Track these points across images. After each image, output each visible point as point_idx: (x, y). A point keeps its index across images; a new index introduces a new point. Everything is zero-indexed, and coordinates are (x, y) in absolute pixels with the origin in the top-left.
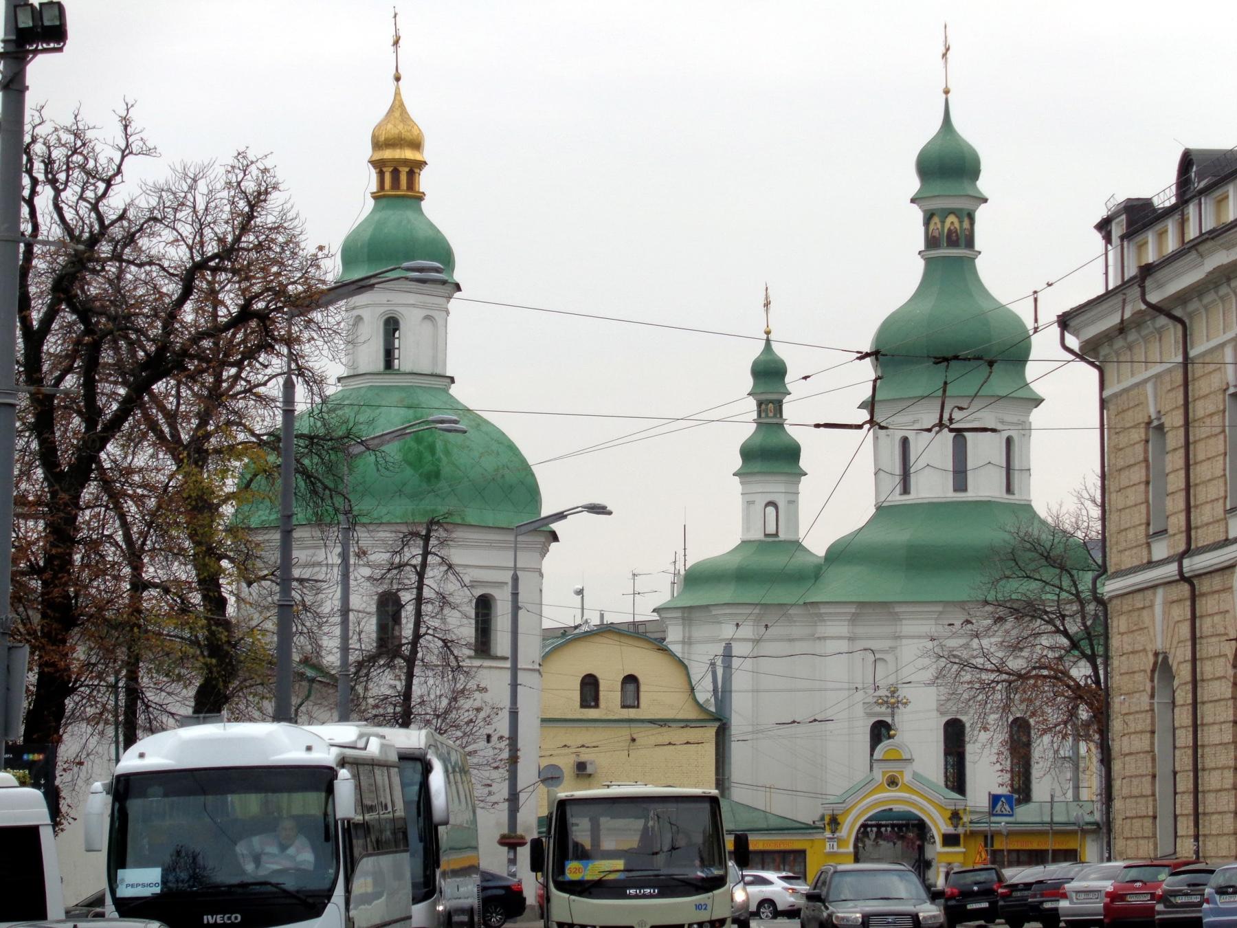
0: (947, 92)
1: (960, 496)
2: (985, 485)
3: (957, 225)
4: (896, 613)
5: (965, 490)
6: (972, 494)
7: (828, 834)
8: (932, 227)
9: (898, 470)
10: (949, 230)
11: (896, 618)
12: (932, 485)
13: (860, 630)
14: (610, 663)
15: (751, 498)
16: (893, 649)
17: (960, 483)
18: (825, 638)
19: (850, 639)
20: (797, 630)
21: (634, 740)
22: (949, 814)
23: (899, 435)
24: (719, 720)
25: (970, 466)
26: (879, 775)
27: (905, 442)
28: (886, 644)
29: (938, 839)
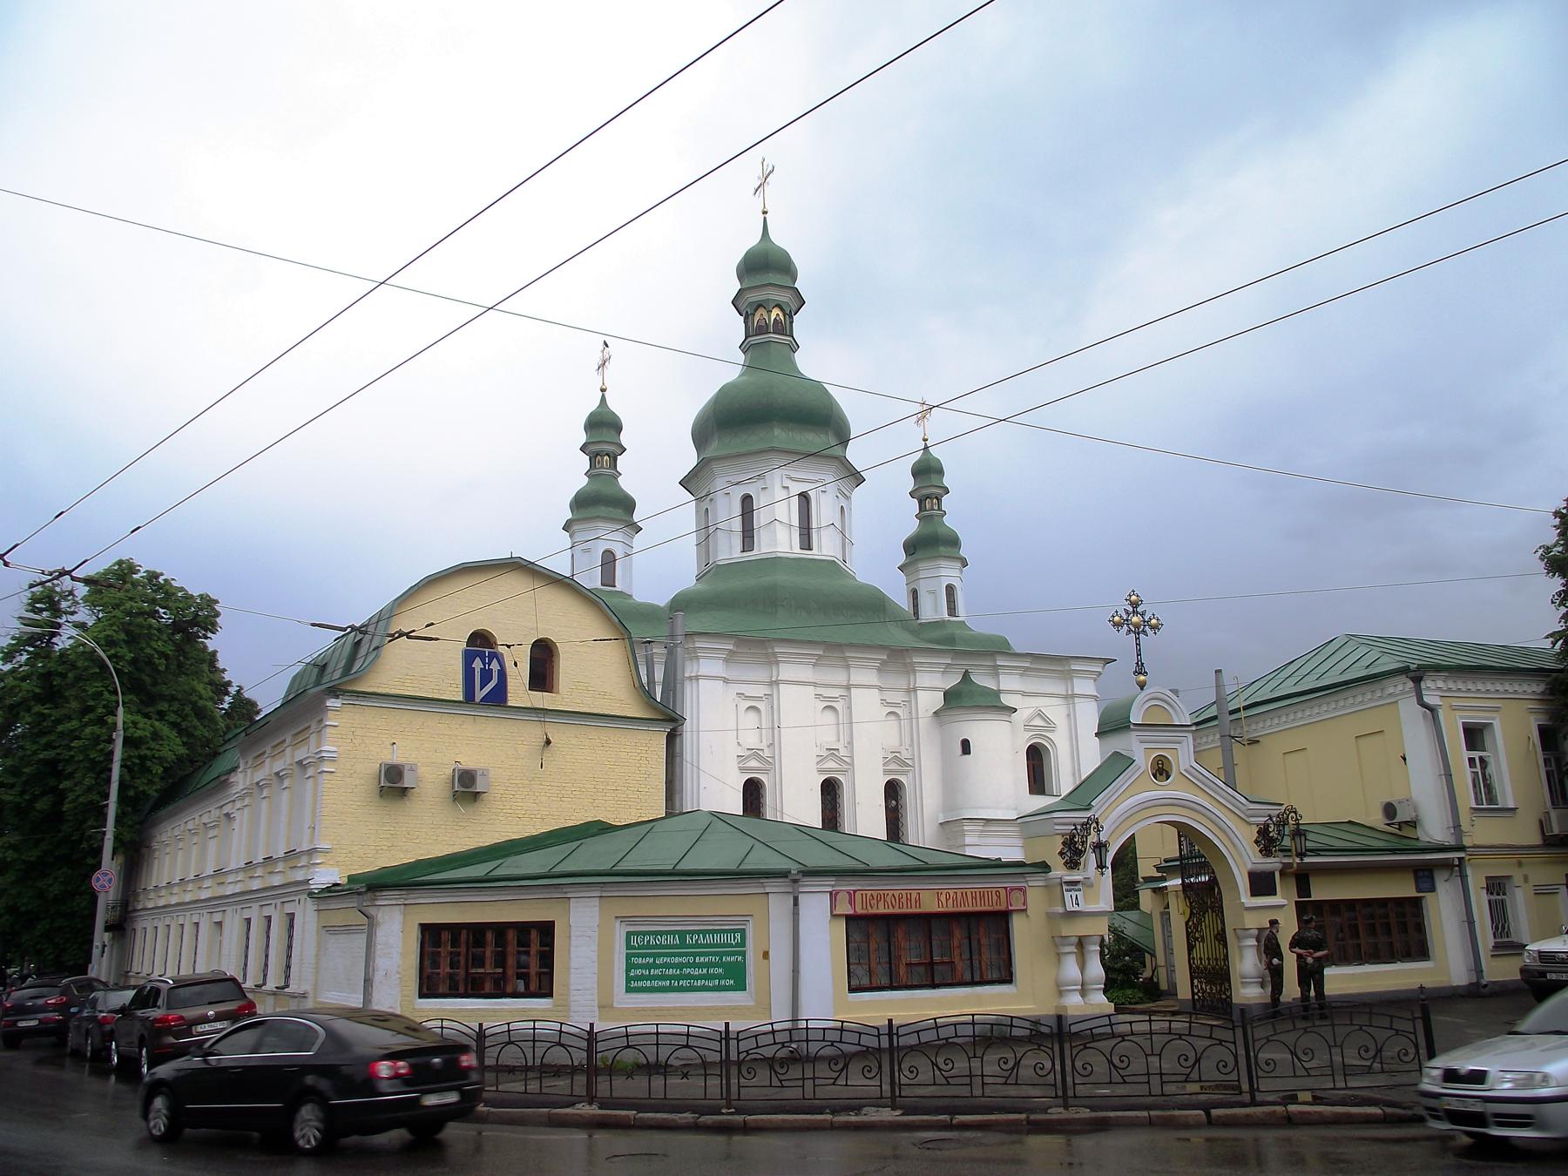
1: (806, 554)
2: (826, 547)
4: (774, 654)
6: (814, 554)
7: (1059, 871)
11: (772, 661)
12: (778, 539)
14: (517, 620)
17: (806, 544)
18: (697, 678)
19: (726, 681)
21: (548, 742)
22: (1253, 833)
23: (737, 494)
24: (673, 720)
26: (1143, 761)
27: (747, 500)
29: (1243, 883)
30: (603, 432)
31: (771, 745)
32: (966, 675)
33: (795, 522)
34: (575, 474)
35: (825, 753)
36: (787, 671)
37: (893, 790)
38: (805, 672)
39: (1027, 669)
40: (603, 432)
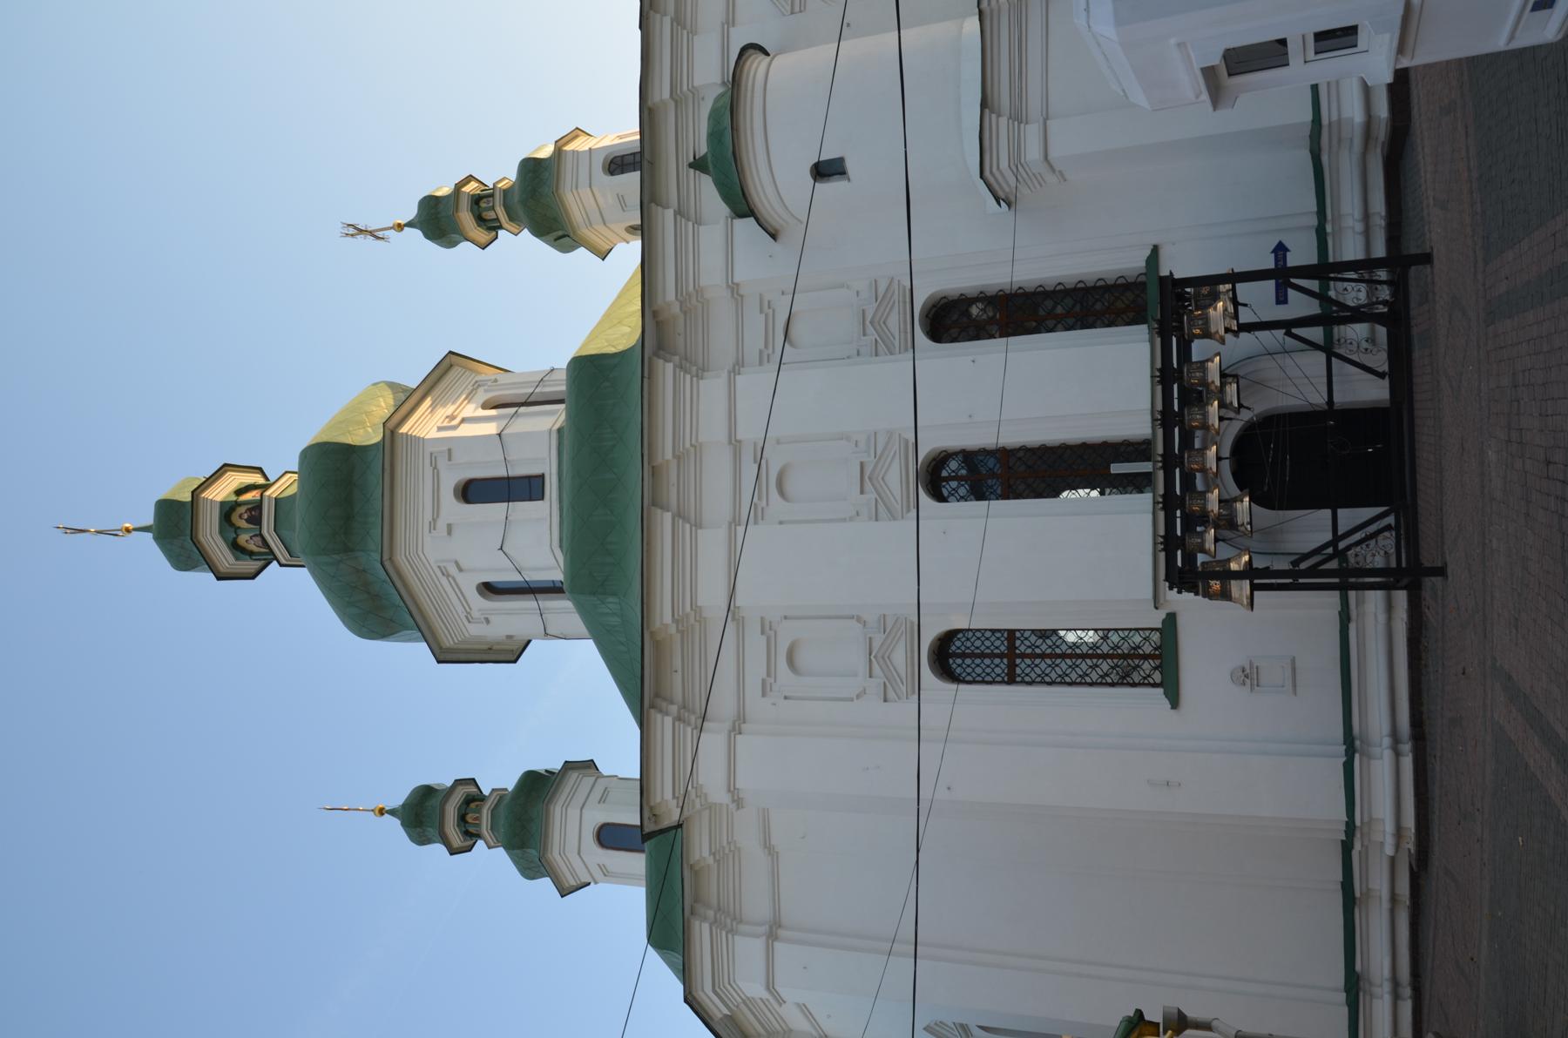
0: (128, 530)
3: (242, 509)
5: (542, 476)
8: (255, 549)
9: (527, 603)
10: (248, 521)
13: (723, 703)
15: (597, 874)
16: (766, 628)
18: (732, 789)
19: (736, 729)
20: (747, 838)
23: (479, 603)
25: (502, 473)
28: (756, 645)
30: (434, 815)
31: (859, 619)
32: (699, 165)
33: (497, 510)
34: (491, 861)
35: (871, 495)
36: (711, 595)
37: (950, 320)
38: (711, 546)
39: (678, 21)
40: (434, 815)
